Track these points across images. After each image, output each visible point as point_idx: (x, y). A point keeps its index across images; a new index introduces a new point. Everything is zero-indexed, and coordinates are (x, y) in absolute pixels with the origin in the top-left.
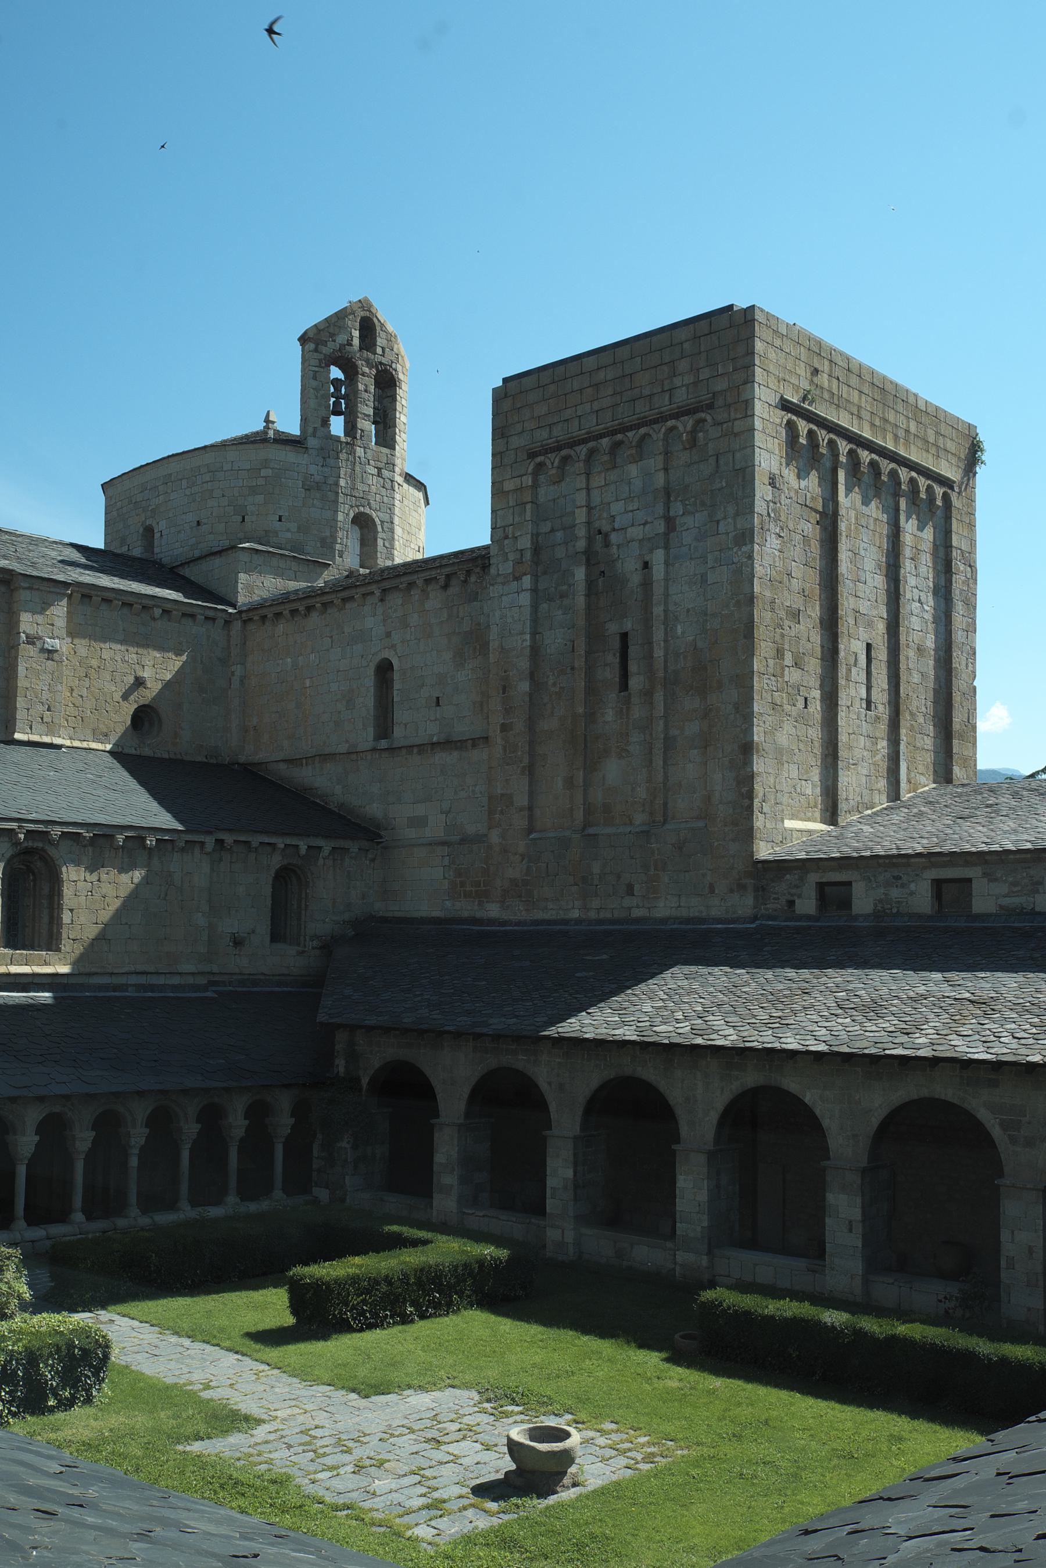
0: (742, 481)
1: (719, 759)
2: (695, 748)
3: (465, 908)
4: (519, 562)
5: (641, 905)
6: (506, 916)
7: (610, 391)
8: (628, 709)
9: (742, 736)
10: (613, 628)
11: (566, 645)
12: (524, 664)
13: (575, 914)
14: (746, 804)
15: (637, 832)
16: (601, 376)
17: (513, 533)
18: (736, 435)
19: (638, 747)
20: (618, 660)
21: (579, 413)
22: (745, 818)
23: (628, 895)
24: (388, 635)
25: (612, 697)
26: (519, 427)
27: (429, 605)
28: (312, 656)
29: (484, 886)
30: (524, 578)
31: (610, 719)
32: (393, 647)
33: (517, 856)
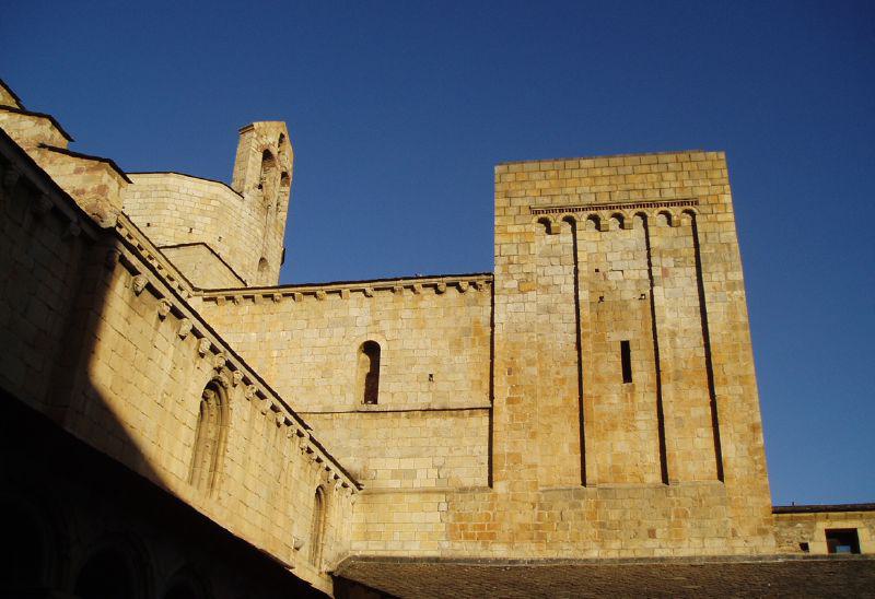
2: (701, 427)
3: (467, 549)
4: (520, 282)
5: (664, 546)
6: (514, 555)
8: (632, 395)
10: (616, 338)
13: (594, 554)
16: (598, 172)
18: (719, 223)
21: (578, 192)
24: (376, 323)
25: (619, 384)
27: (422, 304)
28: (283, 334)
29: (489, 529)
31: (616, 402)
32: (382, 333)
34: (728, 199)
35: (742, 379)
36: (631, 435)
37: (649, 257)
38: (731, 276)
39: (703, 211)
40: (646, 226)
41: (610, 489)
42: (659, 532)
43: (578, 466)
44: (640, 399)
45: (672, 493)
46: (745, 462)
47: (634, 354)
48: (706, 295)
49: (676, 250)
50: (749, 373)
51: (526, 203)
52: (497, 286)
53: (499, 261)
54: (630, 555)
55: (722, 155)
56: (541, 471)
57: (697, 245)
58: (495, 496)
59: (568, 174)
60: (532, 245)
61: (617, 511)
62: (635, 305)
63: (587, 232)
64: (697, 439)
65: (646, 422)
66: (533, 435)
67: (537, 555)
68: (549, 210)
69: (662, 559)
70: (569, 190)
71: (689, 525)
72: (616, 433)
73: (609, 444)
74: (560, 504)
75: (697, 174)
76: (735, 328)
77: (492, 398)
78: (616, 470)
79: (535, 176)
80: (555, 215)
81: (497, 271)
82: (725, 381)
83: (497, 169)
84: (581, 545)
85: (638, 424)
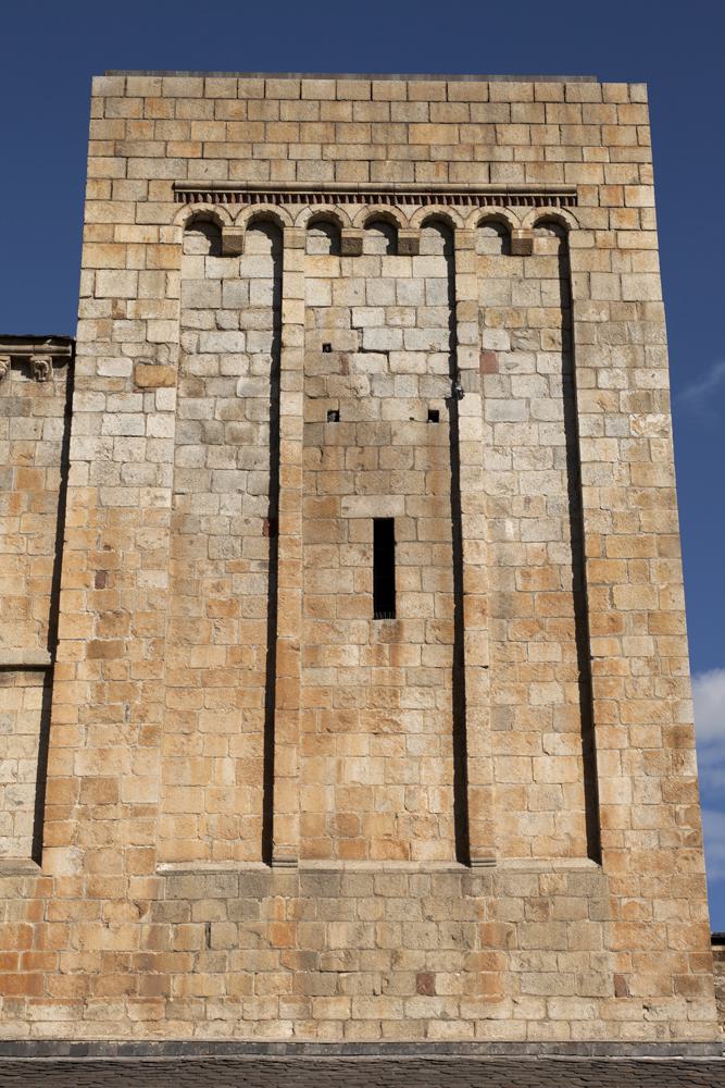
0: (640, 319)
1: (621, 750)
2: (556, 731)
4: (141, 363)
5: (453, 1013)
6: (85, 1033)
7: (363, 137)
8: (395, 650)
9: (669, 714)
10: (363, 508)
11: (247, 521)
12: (159, 540)
13: (282, 1032)
14: (687, 833)
15: (438, 872)
16: (344, 111)
17: (136, 312)
18: (622, 251)
19: (420, 719)
20: (372, 564)
22: (686, 858)
23: (420, 992)
25: (361, 623)
26: (157, 149)
29: (26, 965)
30: (161, 392)
31: (354, 663)
33: (126, 906)
34: (646, 197)
35: (653, 621)
36: (387, 744)
37: (453, 323)
38: (641, 378)
39: (589, 223)
40: (450, 253)
41: (336, 871)
42: (442, 983)
43: (253, 811)
44: (412, 657)
45: (476, 886)
46: (652, 818)
47: (403, 552)
48: (582, 420)
49: (517, 310)
50: (671, 607)
51: (169, 171)
52: (81, 368)
53: (87, 309)
54: (370, 1035)
55: (640, 92)
56: (166, 824)
57: (567, 303)
58: (47, 883)
59: (272, 110)
60: (172, 276)
61: (344, 927)
62: (412, 434)
63: (311, 265)
64: (548, 759)
65: (423, 714)
66: (150, 736)
67: (141, 1033)
68: (217, 193)
69: (446, 1047)
70: (269, 150)
71: (514, 966)
72: (349, 737)
73: (333, 763)
74: (204, 910)
75: (579, 134)
76: (645, 501)
77: (53, 642)
78: (348, 832)
79: (187, 109)
80: (234, 208)
81: (84, 332)
82: (615, 626)
83: (99, 83)
84: (252, 1009)
85: (406, 720)
